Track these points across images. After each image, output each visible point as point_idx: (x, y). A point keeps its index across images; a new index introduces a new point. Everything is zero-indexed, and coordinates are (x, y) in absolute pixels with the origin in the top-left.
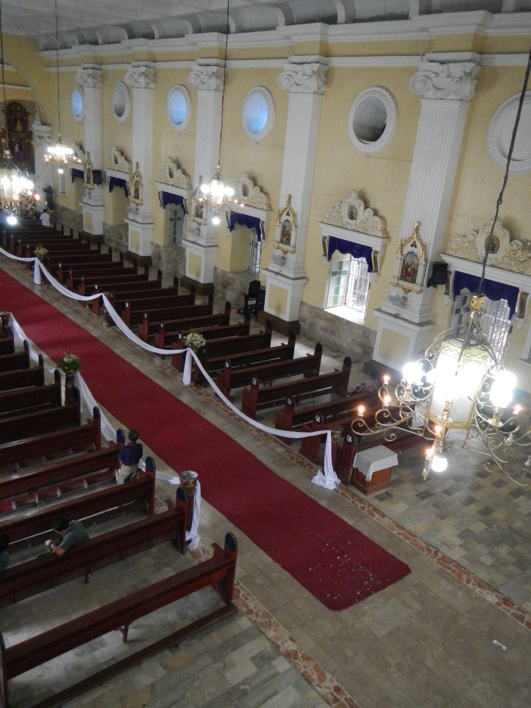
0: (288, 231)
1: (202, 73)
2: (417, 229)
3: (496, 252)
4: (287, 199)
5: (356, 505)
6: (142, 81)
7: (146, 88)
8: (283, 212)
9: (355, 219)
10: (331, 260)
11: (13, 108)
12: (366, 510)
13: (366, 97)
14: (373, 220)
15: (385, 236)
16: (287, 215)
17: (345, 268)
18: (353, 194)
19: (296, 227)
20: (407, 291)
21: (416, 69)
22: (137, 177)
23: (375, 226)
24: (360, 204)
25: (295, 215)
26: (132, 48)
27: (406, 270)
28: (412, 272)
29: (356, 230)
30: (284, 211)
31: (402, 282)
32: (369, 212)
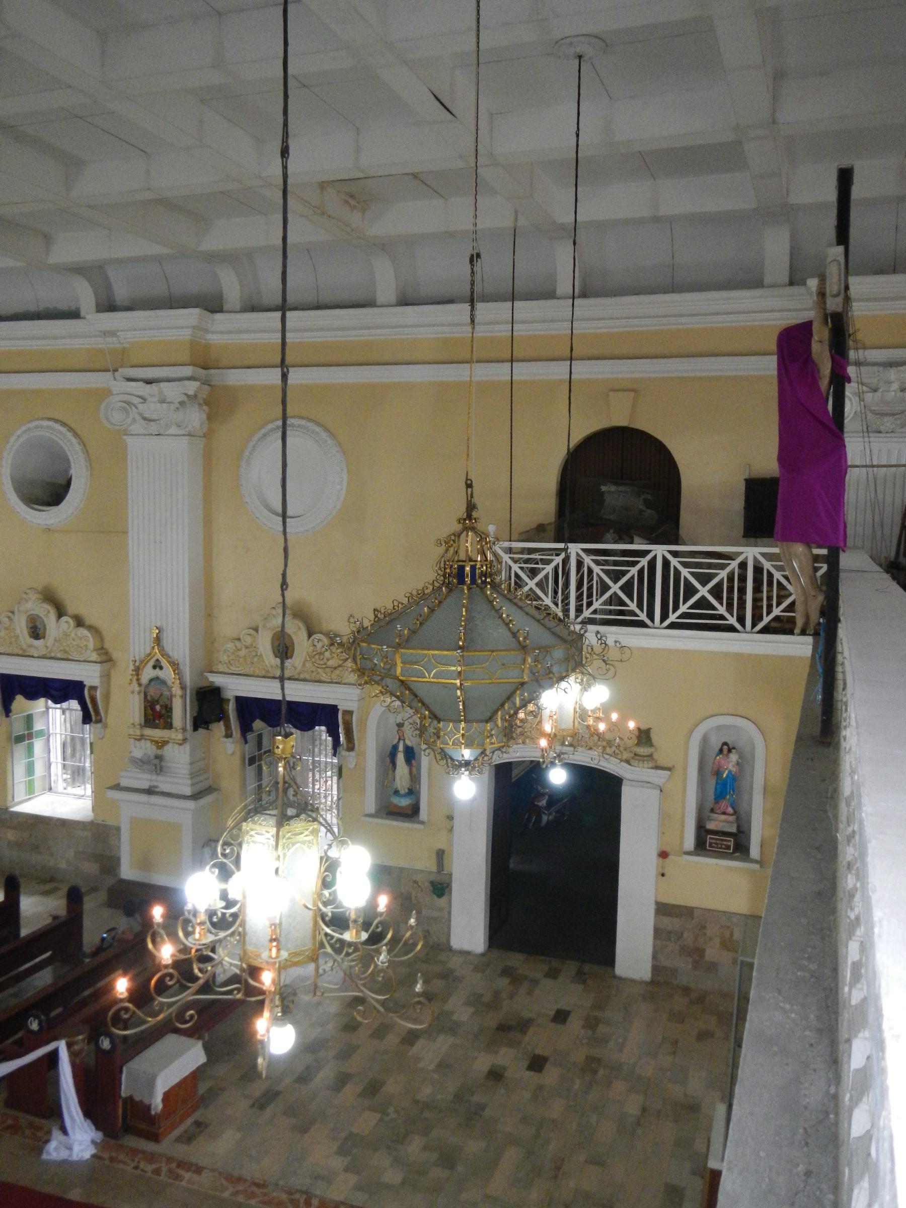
2: (158, 640)
3: (291, 657)
5: (143, 1170)
9: (44, 638)
10: (10, 714)
12: (163, 1173)
13: (26, 437)
14: (76, 635)
15: (104, 658)
17: (38, 726)
21: (106, 393)
23: (82, 645)
27: (153, 708)
28: (163, 711)
29: (48, 655)
31: (148, 732)
32: (67, 622)
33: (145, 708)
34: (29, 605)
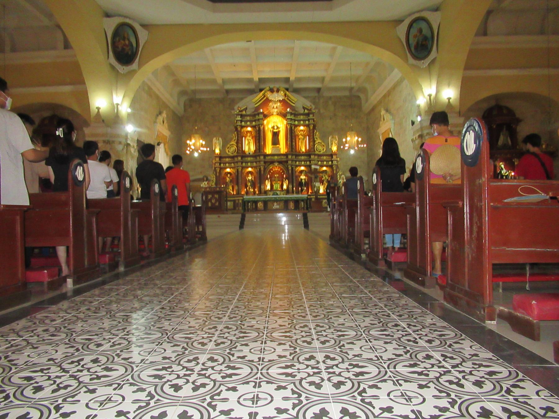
11: (495, 113)
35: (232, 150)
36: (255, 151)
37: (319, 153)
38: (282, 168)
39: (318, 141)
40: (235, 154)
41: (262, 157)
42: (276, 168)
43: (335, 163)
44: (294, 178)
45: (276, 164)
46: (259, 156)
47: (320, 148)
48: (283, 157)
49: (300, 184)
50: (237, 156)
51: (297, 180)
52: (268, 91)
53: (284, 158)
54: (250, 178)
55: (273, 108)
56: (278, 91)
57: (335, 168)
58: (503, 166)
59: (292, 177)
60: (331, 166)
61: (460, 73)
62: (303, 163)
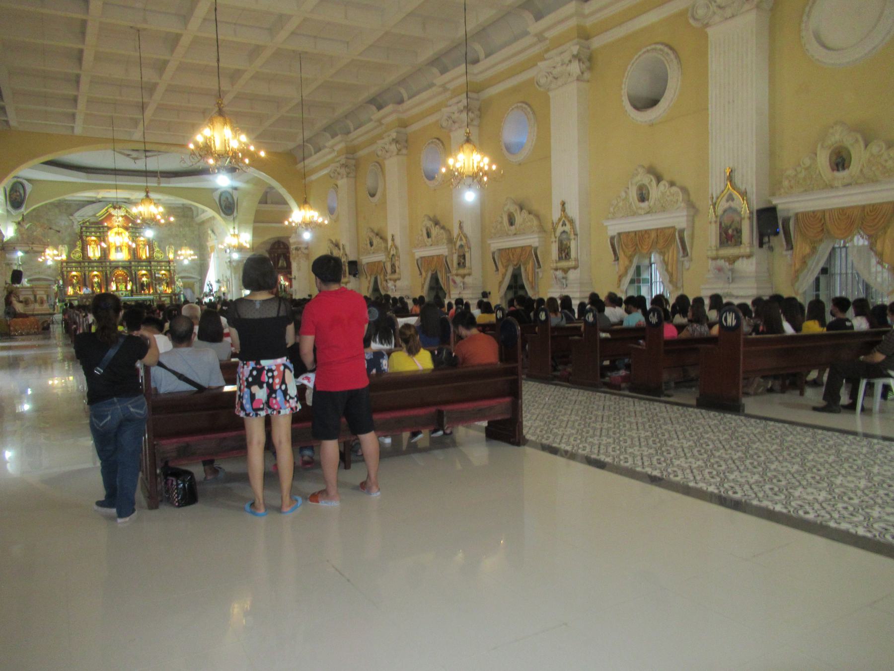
0: (567, 244)
1: (454, 113)
2: (730, 178)
3: (848, 167)
4: (560, 207)
6: (393, 147)
7: (398, 154)
8: (558, 223)
16: (562, 226)
18: (639, 170)
19: (576, 234)
20: (732, 260)
22: (393, 250)
24: (651, 180)
25: (572, 222)
26: (384, 121)
27: (726, 233)
28: (735, 233)
30: (559, 223)
33: (720, 234)
34: (639, 178)
35: (77, 255)
36: (100, 258)
37: (158, 260)
38: (125, 271)
39: (157, 249)
40: (81, 259)
41: (108, 264)
42: (120, 272)
43: (172, 268)
44: (137, 280)
45: (120, 269)
46: (105, 262)
47: (158, 255)
48: (126, 263)
49: (142, 285)
50: (84, 262)
51: (140, 281)
52: (111, 207)
53: (127, 264)
54: (96, 280)
55: (116, 222)
56: (120, 208)
57: (172, 272)
58: (282, 279)
59: (135, 279)
60: (169, 271)
61: (251, 226)
62: (144, 268)
